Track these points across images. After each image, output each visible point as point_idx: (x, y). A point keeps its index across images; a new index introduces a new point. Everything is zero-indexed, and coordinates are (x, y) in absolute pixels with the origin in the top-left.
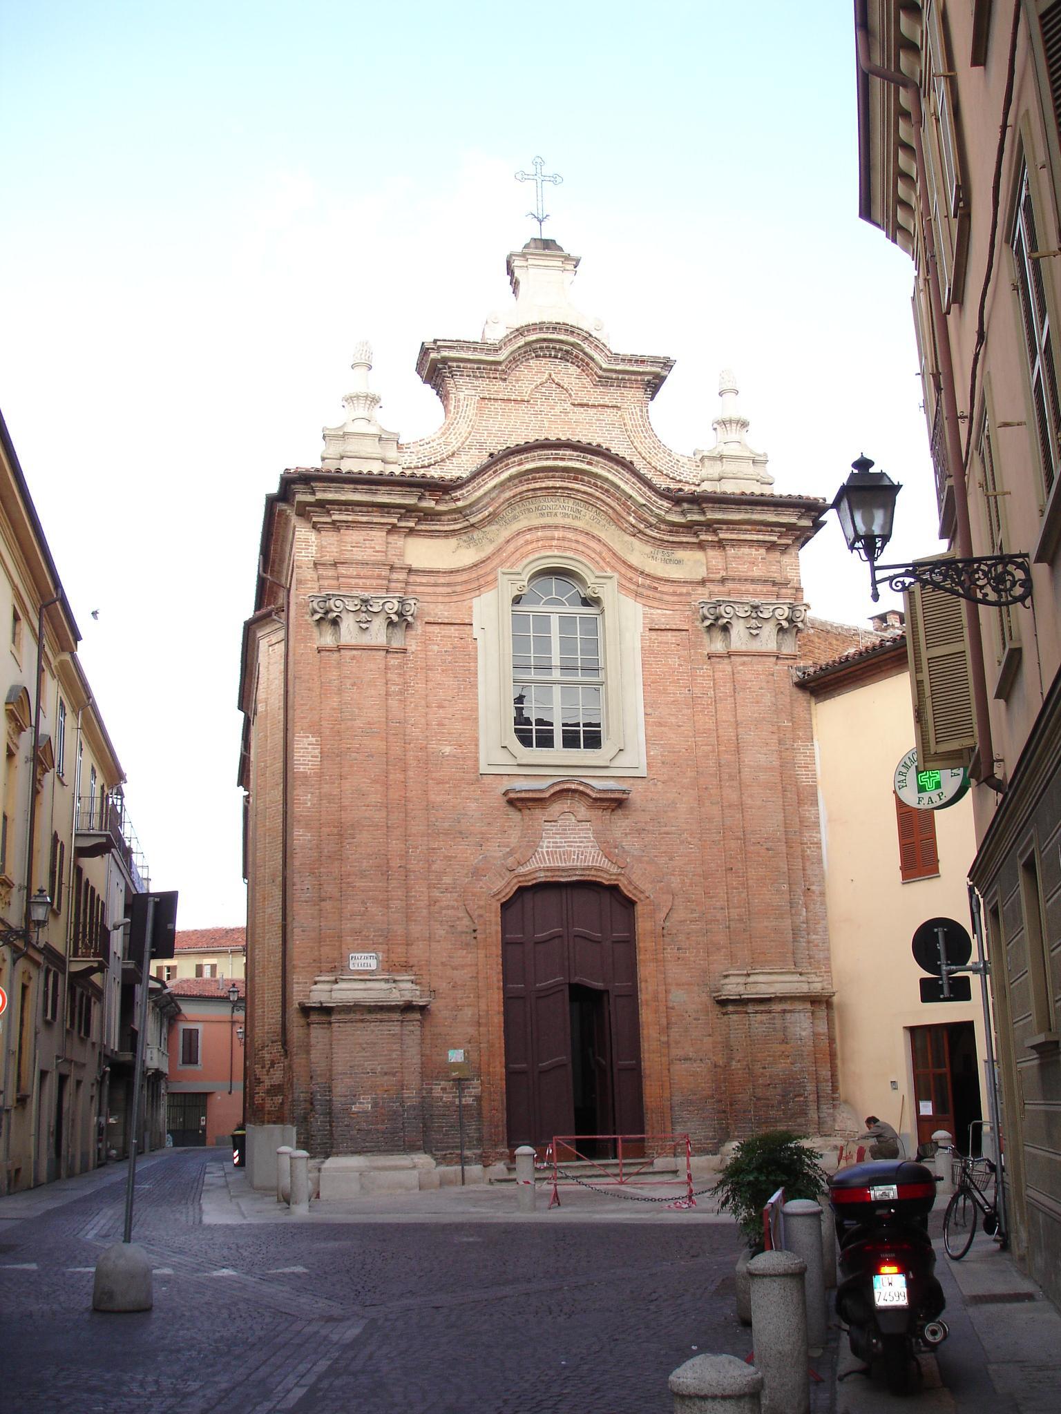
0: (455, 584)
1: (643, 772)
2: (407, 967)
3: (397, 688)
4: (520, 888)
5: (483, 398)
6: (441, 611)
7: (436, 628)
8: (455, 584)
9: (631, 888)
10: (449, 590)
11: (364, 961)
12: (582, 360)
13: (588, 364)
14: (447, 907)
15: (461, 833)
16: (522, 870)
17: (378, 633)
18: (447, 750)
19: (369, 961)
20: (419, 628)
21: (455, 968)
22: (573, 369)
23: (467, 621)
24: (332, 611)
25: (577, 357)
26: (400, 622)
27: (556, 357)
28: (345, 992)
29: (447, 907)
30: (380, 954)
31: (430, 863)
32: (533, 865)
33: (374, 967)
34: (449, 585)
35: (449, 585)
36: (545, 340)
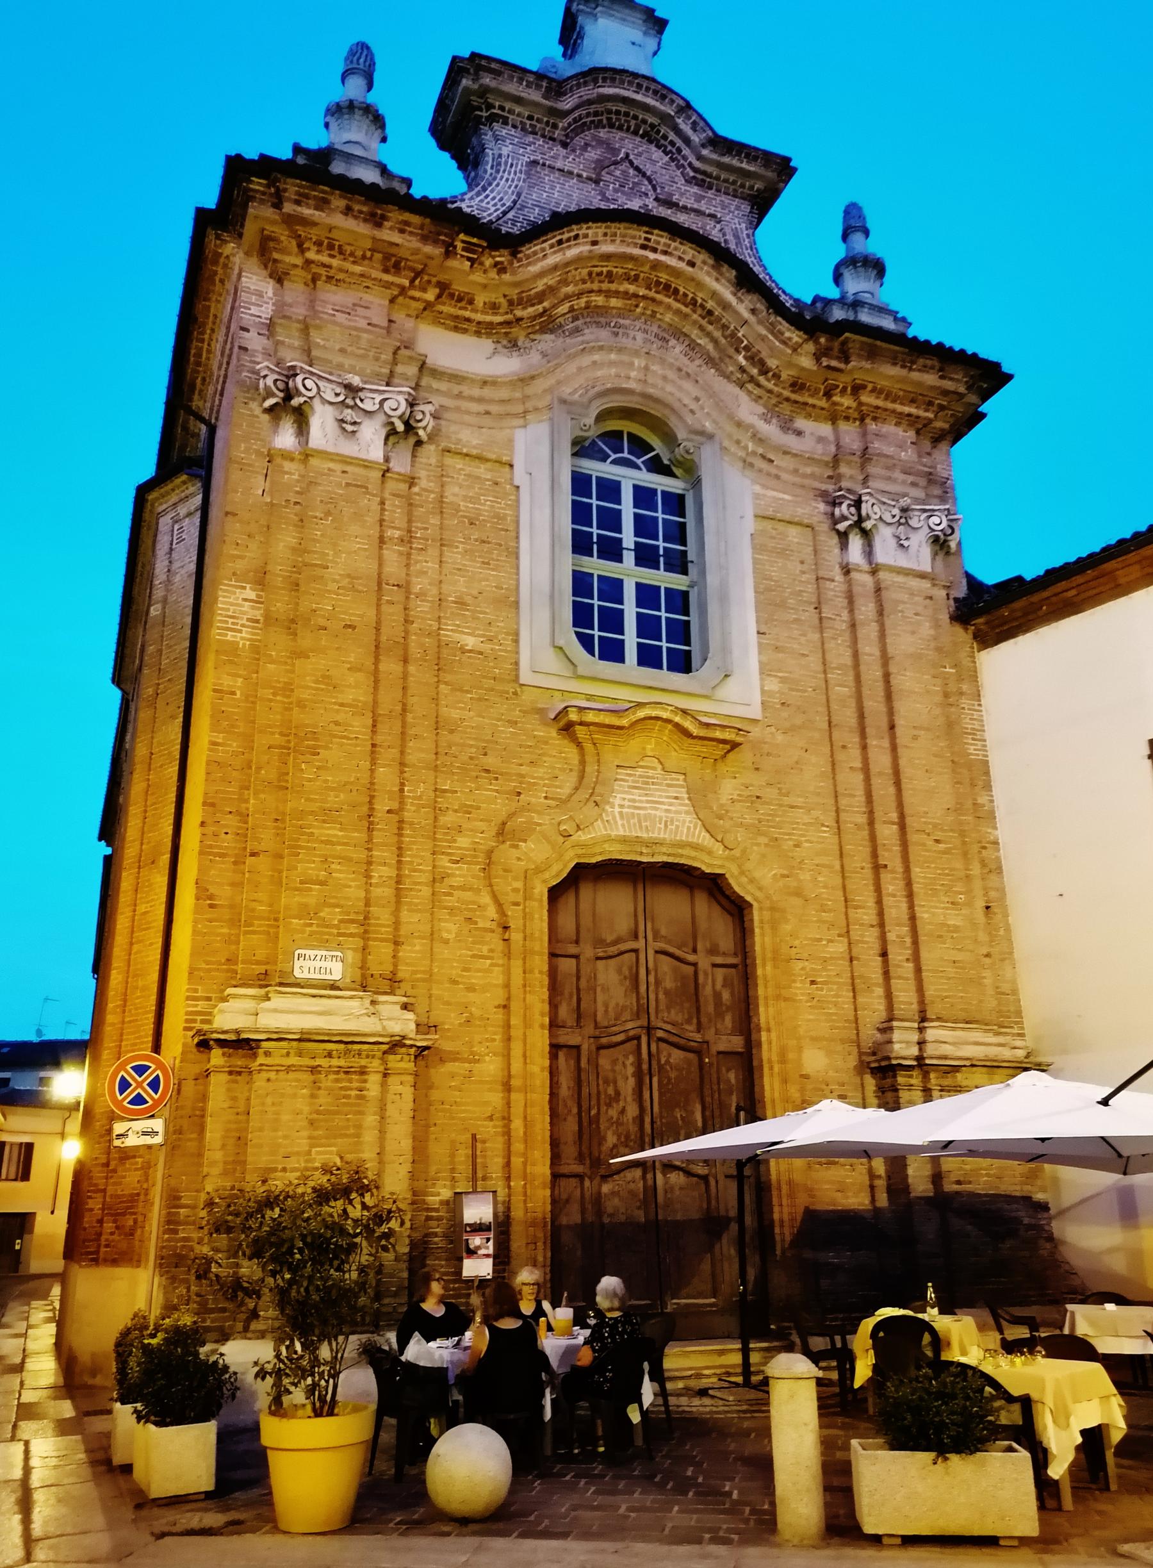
0: (490, 401)
1: (755, 712)
2: (393, 983)
3: (397, 534)
4: (578, 866)
5: (535, 163)
6: (469, 438)
7: (457, 463)
8: (490, 401)
9: (744, 880)
10: (481, 408)
11: (319, 963)
12: (672, 143)
13: (679, 150)
14: (462, 888)
15: (487, 771)
16: (582, 837)
17: (370, 441)
18: (470, 642)
19: (328, 964)
20: (429, 452)
21: (471, 989)
22: (657, 154)
23: (505, 459)
24: (300, 394)
25: (665, 137)
26: (403, 433)
27: (635, 133)
28: (283, 1013)
29: (462, 888)
30: (350, 955)
31: (437, 811)
32: (599, 830)
33: (337, 975)
34: (480, 400)
35: (480, 400)
36: (625, 100)
